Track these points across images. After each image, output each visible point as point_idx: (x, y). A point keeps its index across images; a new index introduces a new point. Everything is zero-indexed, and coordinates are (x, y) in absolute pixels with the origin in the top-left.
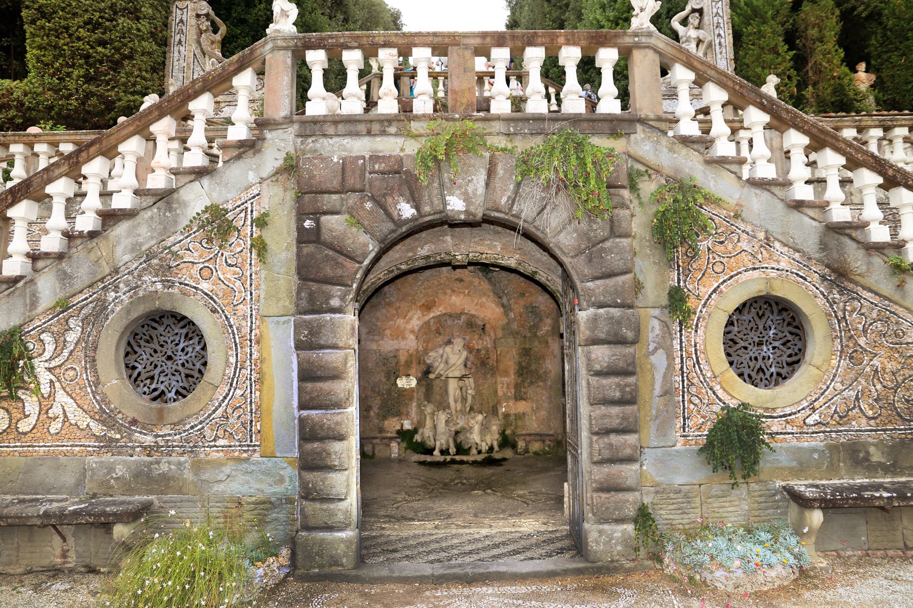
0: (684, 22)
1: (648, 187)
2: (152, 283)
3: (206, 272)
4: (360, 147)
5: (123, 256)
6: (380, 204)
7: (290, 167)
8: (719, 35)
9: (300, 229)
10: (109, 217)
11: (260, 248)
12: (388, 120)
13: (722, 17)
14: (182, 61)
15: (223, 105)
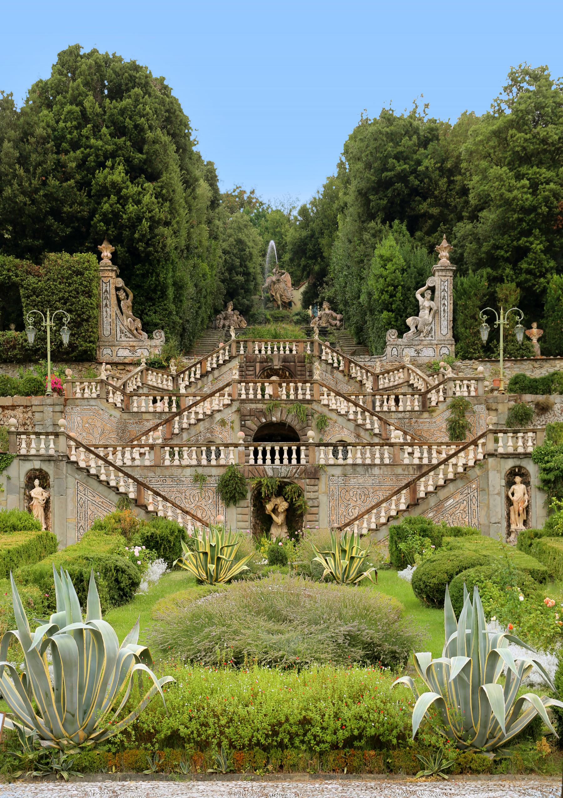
0: (423, 295)
1: (316, 416)
2: (208, 435)
3: (221, 433)
4: (253, 406)
5: (202, 429)
6: (258, 419)
7: (238, 411)
8: (444, 304)
9: (241, 424)
10: (199, 420)
11: (232, 428)
12: (259, 400)
13: (447, 292)
14: (108, 318)
15: (137, 348)
